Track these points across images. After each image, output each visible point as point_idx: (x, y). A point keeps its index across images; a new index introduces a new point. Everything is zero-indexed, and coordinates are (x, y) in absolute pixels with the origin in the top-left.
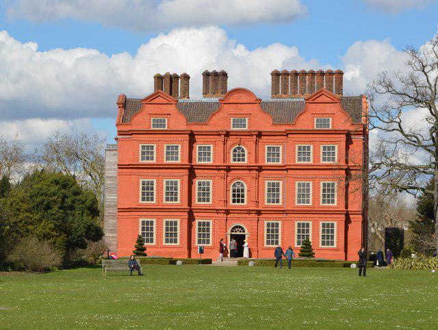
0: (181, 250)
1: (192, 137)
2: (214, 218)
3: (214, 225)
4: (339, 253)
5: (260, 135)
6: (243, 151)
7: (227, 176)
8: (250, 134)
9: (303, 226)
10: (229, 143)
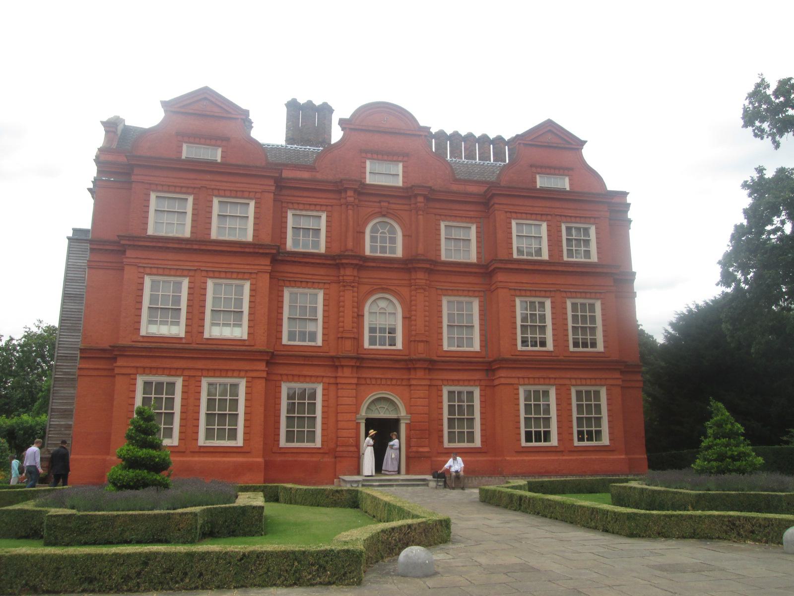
0: (240, 459)
2: (325, 380)
6: (392, 231)
9: (537, 399)
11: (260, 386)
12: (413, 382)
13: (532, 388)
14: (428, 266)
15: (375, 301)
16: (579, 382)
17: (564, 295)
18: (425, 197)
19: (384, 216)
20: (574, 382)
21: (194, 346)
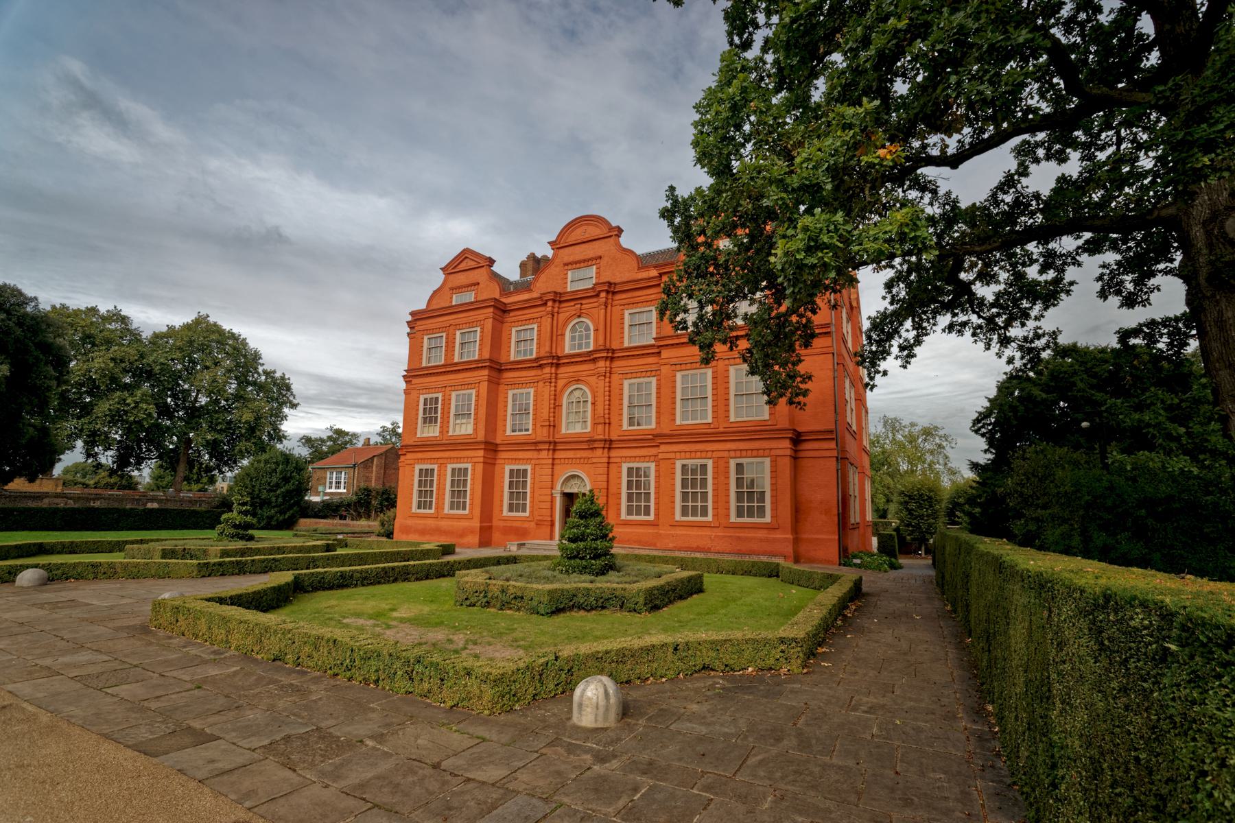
1: (502, 310)
2: (533, 462)
3: (534, 474)
4: (778, 535)
5: (611, 289)
6: (587, 329)
7: (556, 379)
8: (594, 294)
10: (562, 317)
11: (480, 467)
12: (594, 460)
13: (689, 462)
14: (605, 355)
15: (572, 392)
16: (738, 453)
17: (727, 362)
18: (608, 292)
19: (579, 316)
20: (732, 454)
21: (444, 442)
